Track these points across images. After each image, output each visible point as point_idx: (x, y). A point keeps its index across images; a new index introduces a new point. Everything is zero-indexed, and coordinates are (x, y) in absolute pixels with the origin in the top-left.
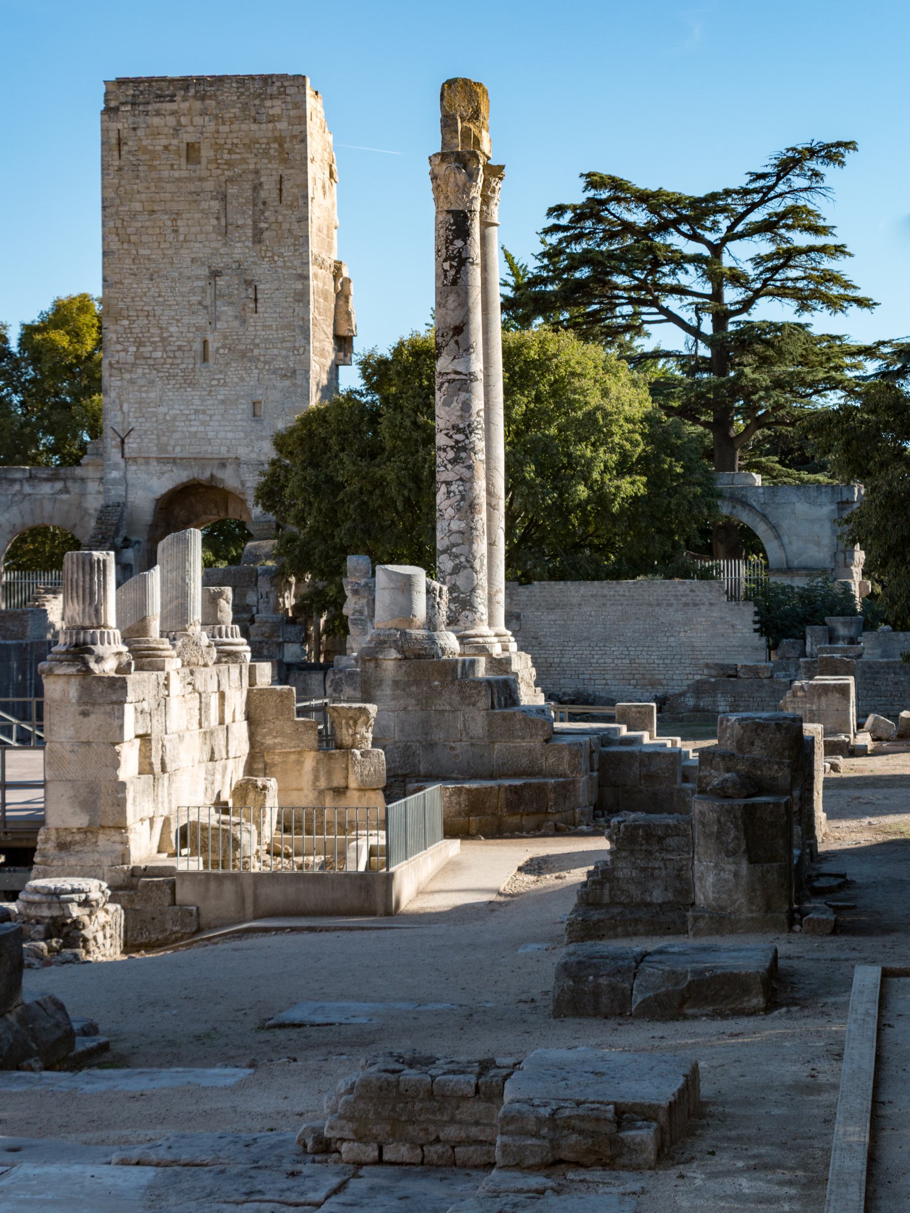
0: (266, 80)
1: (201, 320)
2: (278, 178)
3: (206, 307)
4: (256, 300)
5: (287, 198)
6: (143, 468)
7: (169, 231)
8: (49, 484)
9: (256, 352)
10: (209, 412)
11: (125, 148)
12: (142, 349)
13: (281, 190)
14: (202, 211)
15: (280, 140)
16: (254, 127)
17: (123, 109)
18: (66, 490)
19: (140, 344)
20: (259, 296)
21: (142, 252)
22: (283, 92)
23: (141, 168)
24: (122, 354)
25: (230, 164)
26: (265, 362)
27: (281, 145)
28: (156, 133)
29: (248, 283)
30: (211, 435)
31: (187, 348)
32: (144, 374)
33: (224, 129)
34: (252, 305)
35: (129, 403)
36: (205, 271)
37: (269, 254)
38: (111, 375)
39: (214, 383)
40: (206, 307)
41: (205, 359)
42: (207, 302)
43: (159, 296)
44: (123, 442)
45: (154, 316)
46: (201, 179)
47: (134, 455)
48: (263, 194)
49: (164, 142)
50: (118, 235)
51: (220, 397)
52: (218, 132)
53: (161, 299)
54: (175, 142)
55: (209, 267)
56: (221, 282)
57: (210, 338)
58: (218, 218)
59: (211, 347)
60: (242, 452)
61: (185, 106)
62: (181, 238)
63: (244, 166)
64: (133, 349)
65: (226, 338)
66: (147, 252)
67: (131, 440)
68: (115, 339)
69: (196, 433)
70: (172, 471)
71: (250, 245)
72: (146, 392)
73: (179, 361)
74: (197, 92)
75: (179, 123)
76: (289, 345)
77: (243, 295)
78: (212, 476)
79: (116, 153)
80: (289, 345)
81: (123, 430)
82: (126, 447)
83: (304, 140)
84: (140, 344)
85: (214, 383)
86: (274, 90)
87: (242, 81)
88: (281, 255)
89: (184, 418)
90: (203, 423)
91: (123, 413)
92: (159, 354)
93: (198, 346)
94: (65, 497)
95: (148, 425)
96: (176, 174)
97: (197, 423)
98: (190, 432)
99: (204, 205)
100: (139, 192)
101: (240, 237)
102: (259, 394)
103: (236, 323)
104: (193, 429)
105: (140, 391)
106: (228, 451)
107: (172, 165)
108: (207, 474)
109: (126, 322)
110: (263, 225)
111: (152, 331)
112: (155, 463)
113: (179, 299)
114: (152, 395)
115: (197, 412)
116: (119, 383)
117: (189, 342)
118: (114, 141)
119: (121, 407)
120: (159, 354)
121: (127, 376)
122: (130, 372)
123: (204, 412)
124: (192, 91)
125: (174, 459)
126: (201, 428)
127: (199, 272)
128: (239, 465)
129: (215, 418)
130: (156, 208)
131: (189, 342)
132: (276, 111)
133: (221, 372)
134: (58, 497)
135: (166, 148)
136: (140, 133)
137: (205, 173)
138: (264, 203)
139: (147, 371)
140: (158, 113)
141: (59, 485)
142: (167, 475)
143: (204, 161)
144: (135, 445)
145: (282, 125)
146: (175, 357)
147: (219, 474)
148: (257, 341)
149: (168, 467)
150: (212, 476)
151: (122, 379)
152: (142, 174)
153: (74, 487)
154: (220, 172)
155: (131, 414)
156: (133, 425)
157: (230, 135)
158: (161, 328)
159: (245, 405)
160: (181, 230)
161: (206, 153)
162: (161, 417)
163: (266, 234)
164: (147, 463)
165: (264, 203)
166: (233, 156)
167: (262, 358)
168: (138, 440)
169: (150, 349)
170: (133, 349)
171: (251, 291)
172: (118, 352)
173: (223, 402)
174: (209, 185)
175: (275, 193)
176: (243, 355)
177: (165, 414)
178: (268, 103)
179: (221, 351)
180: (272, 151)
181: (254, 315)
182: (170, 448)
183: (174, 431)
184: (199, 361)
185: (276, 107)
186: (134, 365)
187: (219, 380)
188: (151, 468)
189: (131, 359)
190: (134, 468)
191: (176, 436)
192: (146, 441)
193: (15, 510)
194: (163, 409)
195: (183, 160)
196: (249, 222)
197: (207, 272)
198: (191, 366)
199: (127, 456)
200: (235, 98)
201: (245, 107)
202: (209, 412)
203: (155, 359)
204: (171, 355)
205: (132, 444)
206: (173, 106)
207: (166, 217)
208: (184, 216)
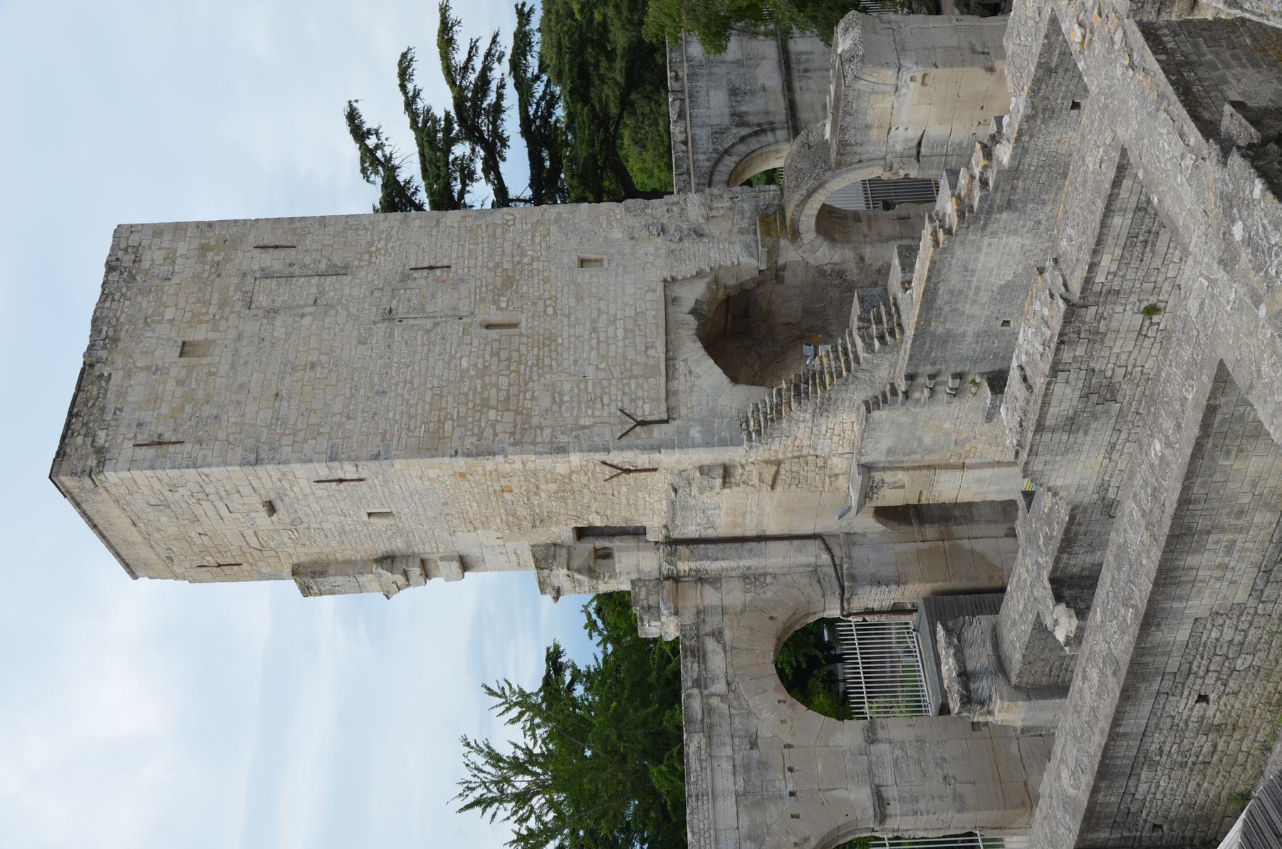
0: (110, 267)
1: (454, 329)
2: (257, 252)
3: (436, 324)
4: (431, 268)
5: (291, 240)
6: (682, 398)
7: (312, 374)
8: (710, 656)
9: (506, 265)
10: (595, 315)
11: (168, 436)
12: (493, 402)
13: (277, 247)
14: (288, 335)
15: (204, 249)
16: (176, 279)
17: (101, 442)
18: (718, 635)
19: (486, 404)
20: (426, 264)
21: (338, 406)
22: (137, 252)
23: (205, 414)
24: (499, 428)
25: (223, 303)
26: (523, 254)
27: (213, 249)
28: (154, 399)
29: (405, 278)
30: (630, 312)
31: (496, 345)
32: (533, 398)
33: (169, 314)
34: (438, 272)
35: (578, 417)
36: (381, 329)
37: (367, 257)
38: (534, 443)
39: (550, 311)
40: (436, 324)
41: (514, 325)
42: (429, 324)
43: (411, 382)
44: (643, 423)
45: (441, 387)
46: (239, 338)
47: (663, 407)
48: (277, 266)
49: (171, 385)
50: (305, 441)
51: (573, 302)
52: (171, 321)
53: (416, 382)
54: (173, 372)
55: (375, 323)
56: (401, 311)
57: (479, 318)
58: (303, 316)
59: (496, 317)
60: (656, 275)
61: (119, 362)
62: (324, 358)
63: (232, 289)
64: (492, 415)
65: (482, 300)
66: (340, 400)
67: (639, 412)
68: (474, 440)
69: (626, 330)
70: (685, 360)
71: (349, 277)
72: (562, 395)
73: (515, 355)
74: (104, 348)
75: (148, 368)
76: (499, 231)
77: (423, 282)
78: (693, 312)
79: (172, 448)
80: (499, 231)
81: (622, 423)
82: (649, 418)
83: (210, 225)
84: (486, 404)
85: (550, 311)
86: (127, 259)
87: (104, 296)
88: (370, 244)
89: (603, 346)
90: (613, 321)
91: (595, 424)
92: (503, 381)
93: (493, 333)
94: (727, 634)
95: (613, 390)
96: (224, 368)
97: (611, 330)
98: (625, 338)
99: (280, 332)
100: (242, 416)
101: (335, 289)
102: (571, 259)
103: (463, 289)
104: (620, 334)
105: (561, 403)
106: (654, 291)
107: (210, 374)
108: (691, 318)
109: (448, 425)
110: (323, 266)
111: (466, 390)
112: (675, 385)
113: (418, 357)
114: (567, 387)
115: (594, 330)
116: (547, 432)
117: (486, 345)
118: (151, 452)
119: (584, 427)
120: (503, 381)
121: (535, 421)
122: (529, 416)
123: (594, 321)
124: (103, 354)
125: (667, 359)
126: (620, 324)
127: (381, 333)
128: (674, 279)
129: (603, 308)
130: (273, 390)
131: (486, 345)
132: (159, 256)
133: (535, 304)
134: (728, 644)
135: (180, 383)
136: (147, 416)
137: (232, 334)
138: (291, 265)
139: (528, 395)
140: (122, 395)
141: (711, 644)
142: (693, 367)
143: (211, 336)
144: (647, 407)
145: (182, 249)
146: (509, 359)
147: (689, 304)
148: (491, 265)
149: (680, 365)
150: (693, 312)
151: (541, 428)
152: (215, 412)
153: (711, 623)
154: (232, 317)
155: (597, 413)
156: (613, 409)
157: (182, 304)
158: (462, 379)
159: (585, 275)
160: (312, 357)
161: (200, 334)
162: (601, 375)
163: (337, 260)
164: (676, 393)
165: (291, 265)
166: (214, 301)
167: (516, 259)
168: (640, 403)
169: (493, 390)
170: (492, 415)
171: (416, 274)
172: (495, 435)
173: (579, 299)
174: (251, 328)
175: (281, 253)
176: (510, 281)
177: (598, 369)
178: (146, 264)
179: (503, 305)
180: (217, 259)
181: (453, 270)
182: (651, 362)
183: (624, 357)
184: (516, 331)
185: (153, 257)
186: (517, 412)
187: (546, 306)
188: (681, 388)
189: (508, 417)
190: (683, 411)
191: (631, 354)
192: (640, 393)
193: (754, 702)
194: (590, 372)
195: (204, 361)
196: (315, 280)
197: (383, 326)
198: (525, 340)
199: (665, 417)
200: (127, 303)
201: (146, 292)
202: (595, 315)
203: (510, 385)
204: (503, 365)
205: (645, 410)
206: (117, 377)
207: (288, 379)
208: (291, 357)
